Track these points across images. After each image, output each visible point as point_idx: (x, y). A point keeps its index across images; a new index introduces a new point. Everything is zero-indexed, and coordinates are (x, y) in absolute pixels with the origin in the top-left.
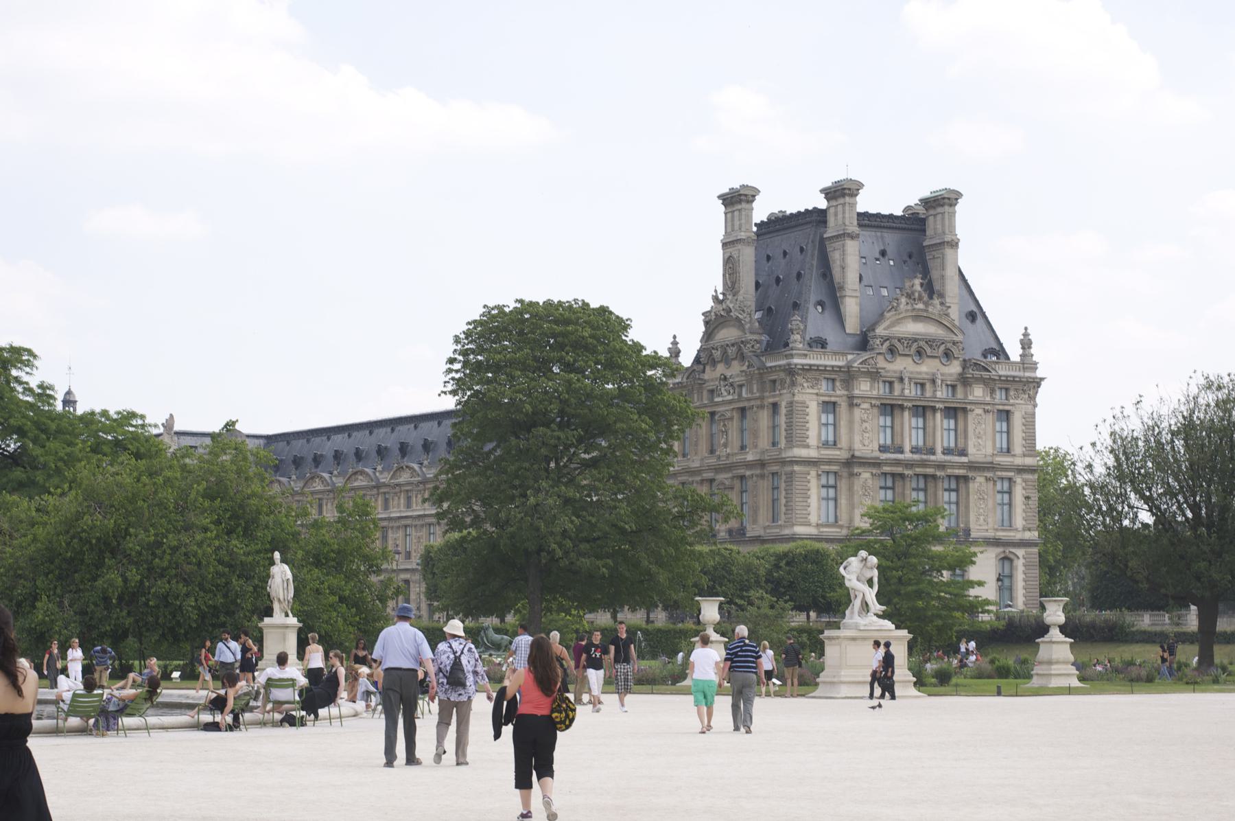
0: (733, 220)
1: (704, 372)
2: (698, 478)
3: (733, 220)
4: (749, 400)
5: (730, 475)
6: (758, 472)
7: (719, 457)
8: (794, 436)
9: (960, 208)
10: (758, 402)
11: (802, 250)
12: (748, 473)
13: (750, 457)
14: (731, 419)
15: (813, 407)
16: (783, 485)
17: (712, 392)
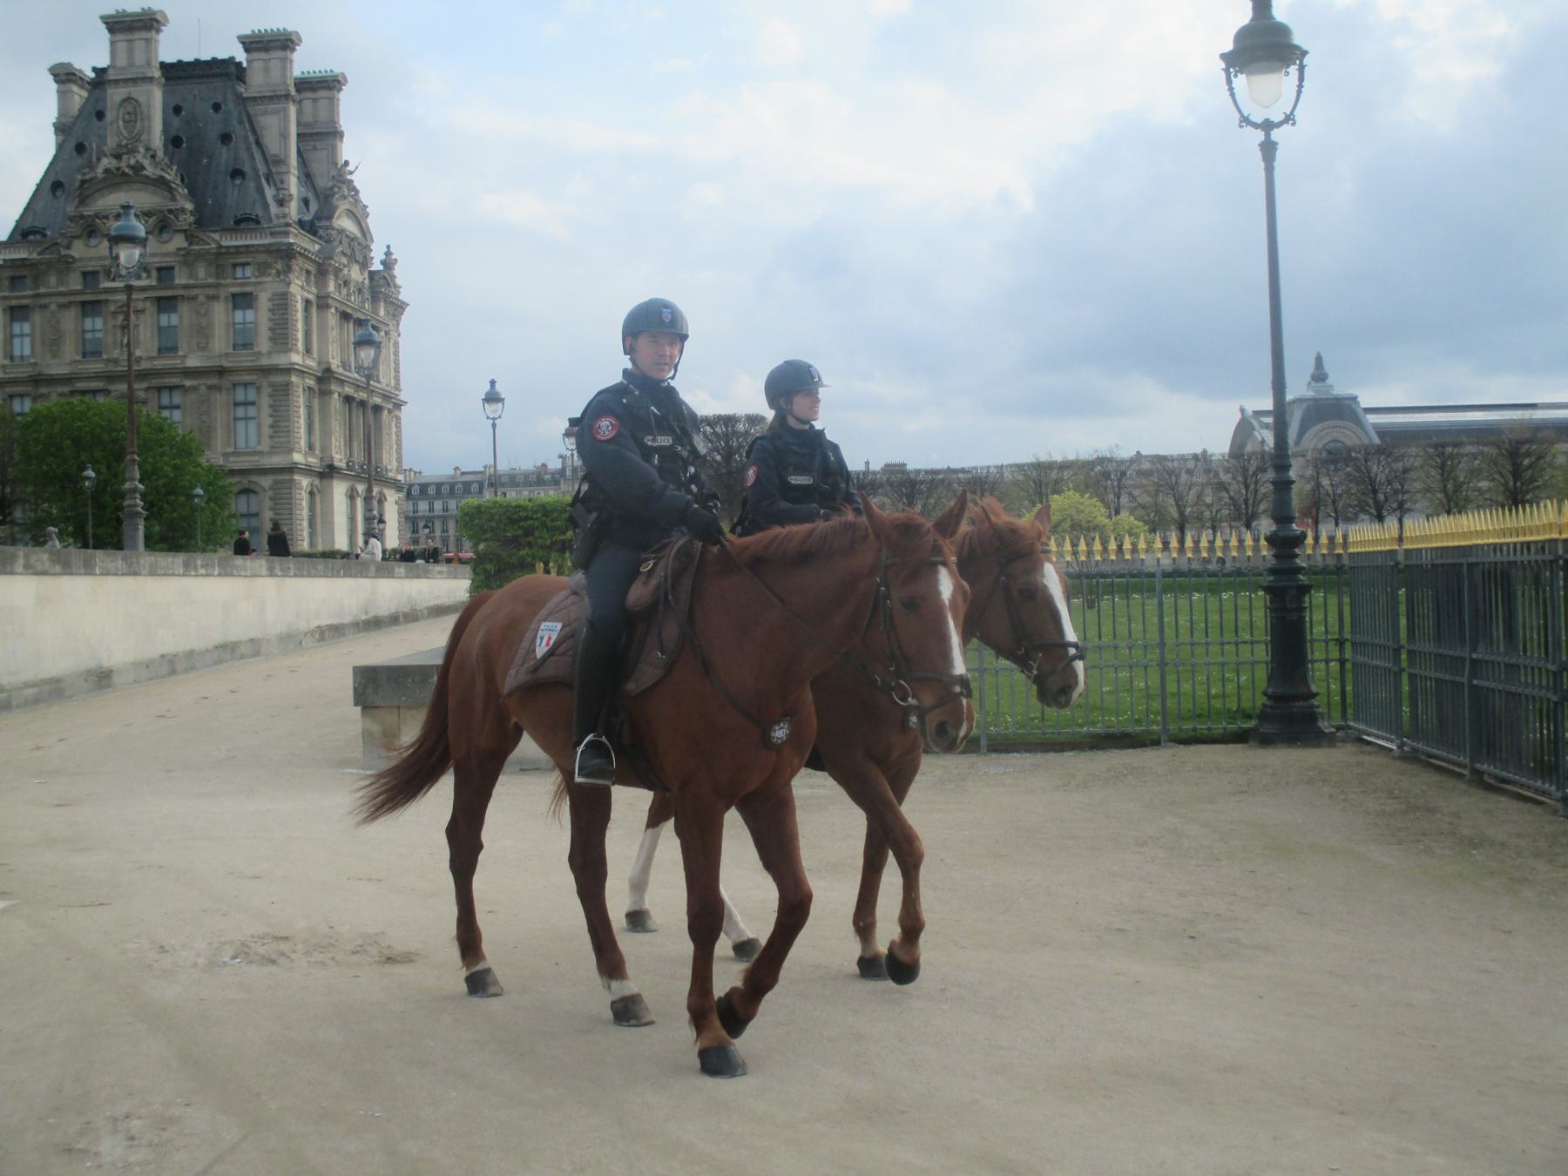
0: (130, 51)
1: (68, 247)
2: (66, 389)
3: (130, 51)
4: (186, 287)
5: (144, 385)
6: (214, 381)
7: (116, 362)
8: (281, 337)
9: (345, 97)
10: (211, 291)
11: (217, 107)
12: (188, 383)
13: (193, 362)
14: (143, 311)
15: (300, 306)
16: (265, 401)
17: (85, 274)
